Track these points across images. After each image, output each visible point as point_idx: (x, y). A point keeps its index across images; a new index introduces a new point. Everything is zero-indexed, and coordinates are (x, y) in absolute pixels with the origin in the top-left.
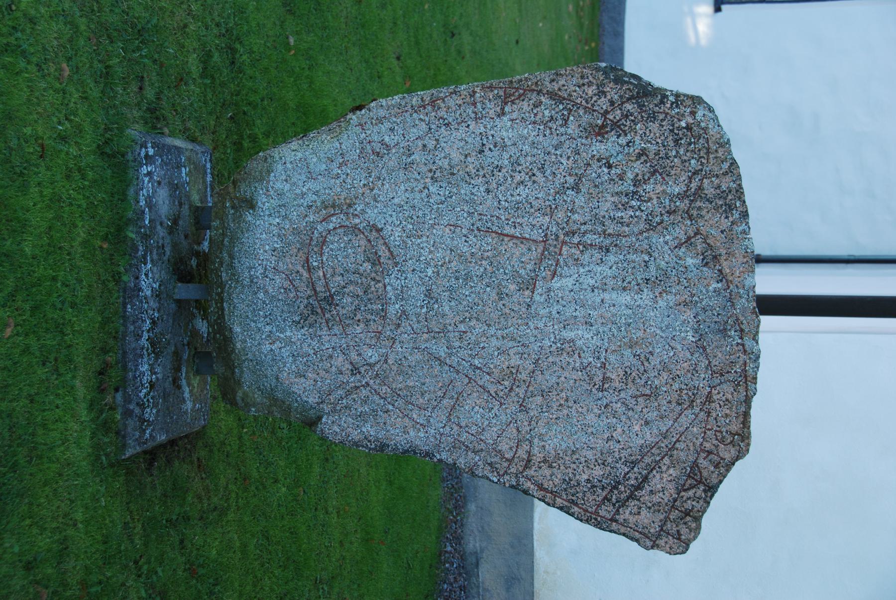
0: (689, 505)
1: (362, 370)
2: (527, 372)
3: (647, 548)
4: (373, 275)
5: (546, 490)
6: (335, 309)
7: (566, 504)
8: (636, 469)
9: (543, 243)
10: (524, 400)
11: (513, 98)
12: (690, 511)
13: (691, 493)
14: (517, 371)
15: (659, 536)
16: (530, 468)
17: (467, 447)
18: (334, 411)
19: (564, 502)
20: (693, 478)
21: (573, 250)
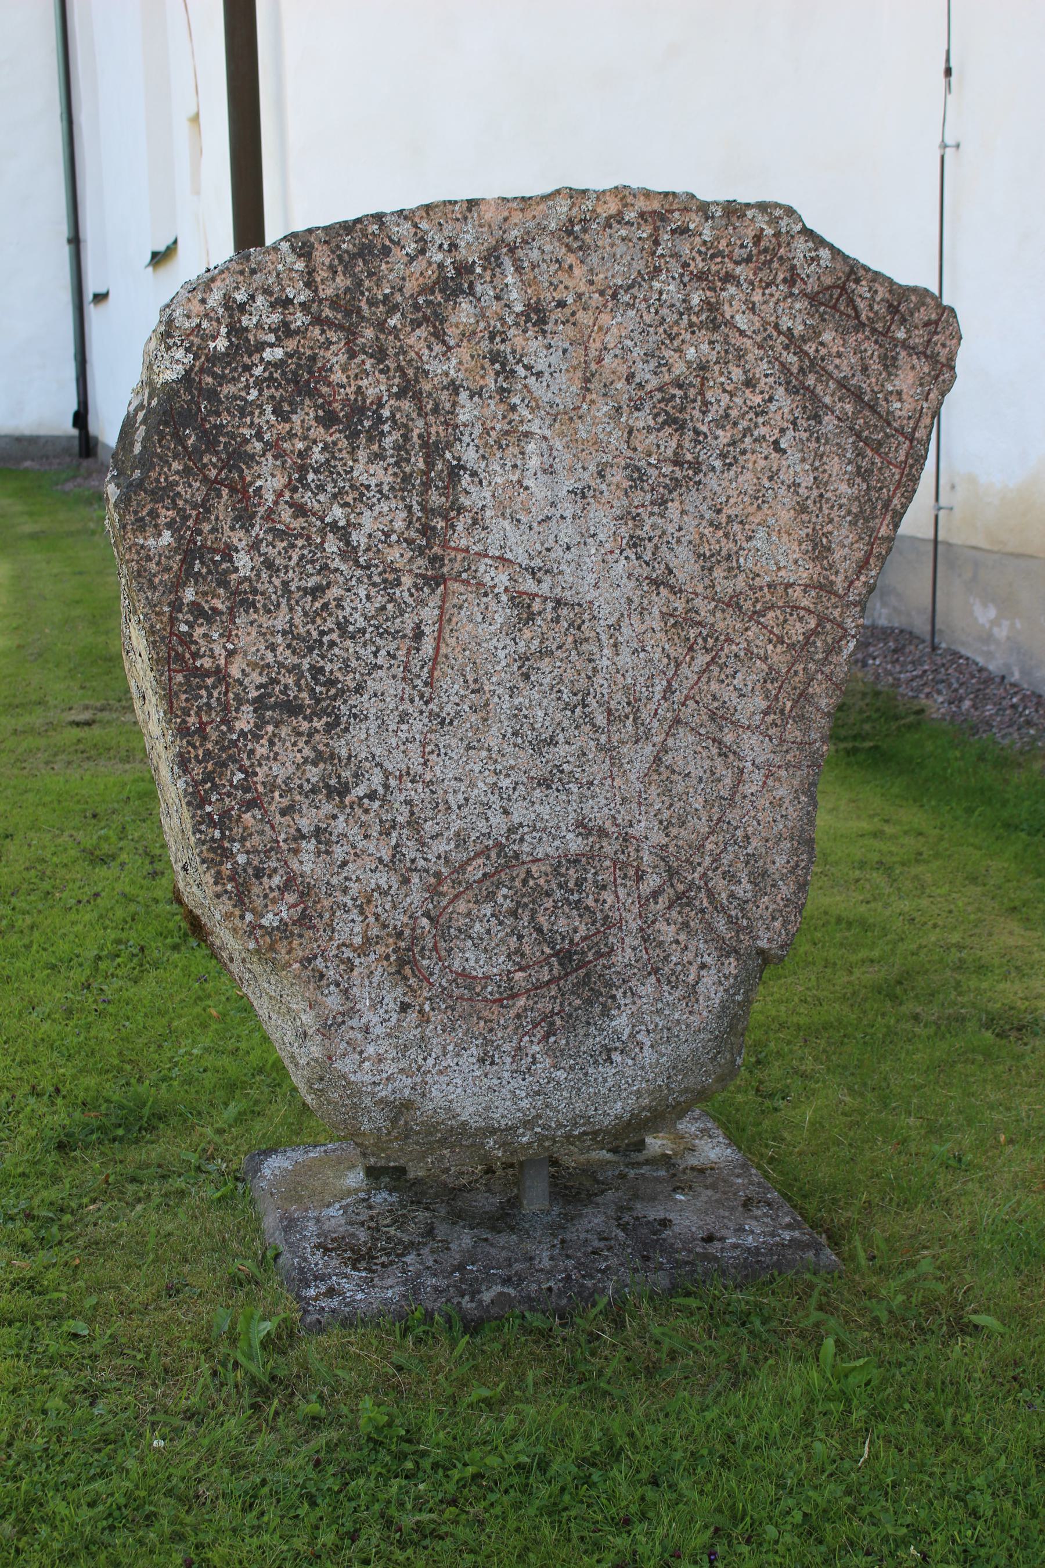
0: (881, 309)
1: (681, 887)
2: (672, 598)
3: (954, 377)
4: (518, 883)
5: (869, 554)
6: (578, 944)
7: (888, 518)
8: (827, 400)
9: (449, 583)
10: (719, 601)
11: (187, 656)
12: (890, 305)
13: (862, 305)
14: (671, 615)
15: (932, 359)
16: (832, 583)
17: (801, 695)
18: (749, 929)
19: (886, 522)
20: (838, 300)
21: (460, 528)
